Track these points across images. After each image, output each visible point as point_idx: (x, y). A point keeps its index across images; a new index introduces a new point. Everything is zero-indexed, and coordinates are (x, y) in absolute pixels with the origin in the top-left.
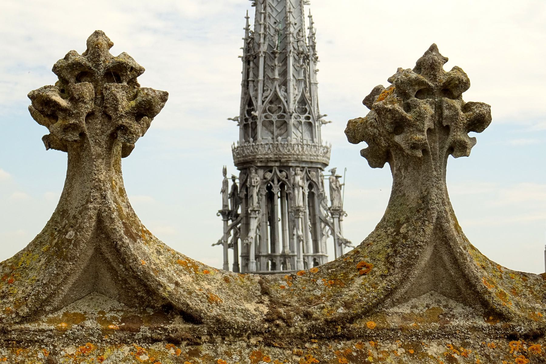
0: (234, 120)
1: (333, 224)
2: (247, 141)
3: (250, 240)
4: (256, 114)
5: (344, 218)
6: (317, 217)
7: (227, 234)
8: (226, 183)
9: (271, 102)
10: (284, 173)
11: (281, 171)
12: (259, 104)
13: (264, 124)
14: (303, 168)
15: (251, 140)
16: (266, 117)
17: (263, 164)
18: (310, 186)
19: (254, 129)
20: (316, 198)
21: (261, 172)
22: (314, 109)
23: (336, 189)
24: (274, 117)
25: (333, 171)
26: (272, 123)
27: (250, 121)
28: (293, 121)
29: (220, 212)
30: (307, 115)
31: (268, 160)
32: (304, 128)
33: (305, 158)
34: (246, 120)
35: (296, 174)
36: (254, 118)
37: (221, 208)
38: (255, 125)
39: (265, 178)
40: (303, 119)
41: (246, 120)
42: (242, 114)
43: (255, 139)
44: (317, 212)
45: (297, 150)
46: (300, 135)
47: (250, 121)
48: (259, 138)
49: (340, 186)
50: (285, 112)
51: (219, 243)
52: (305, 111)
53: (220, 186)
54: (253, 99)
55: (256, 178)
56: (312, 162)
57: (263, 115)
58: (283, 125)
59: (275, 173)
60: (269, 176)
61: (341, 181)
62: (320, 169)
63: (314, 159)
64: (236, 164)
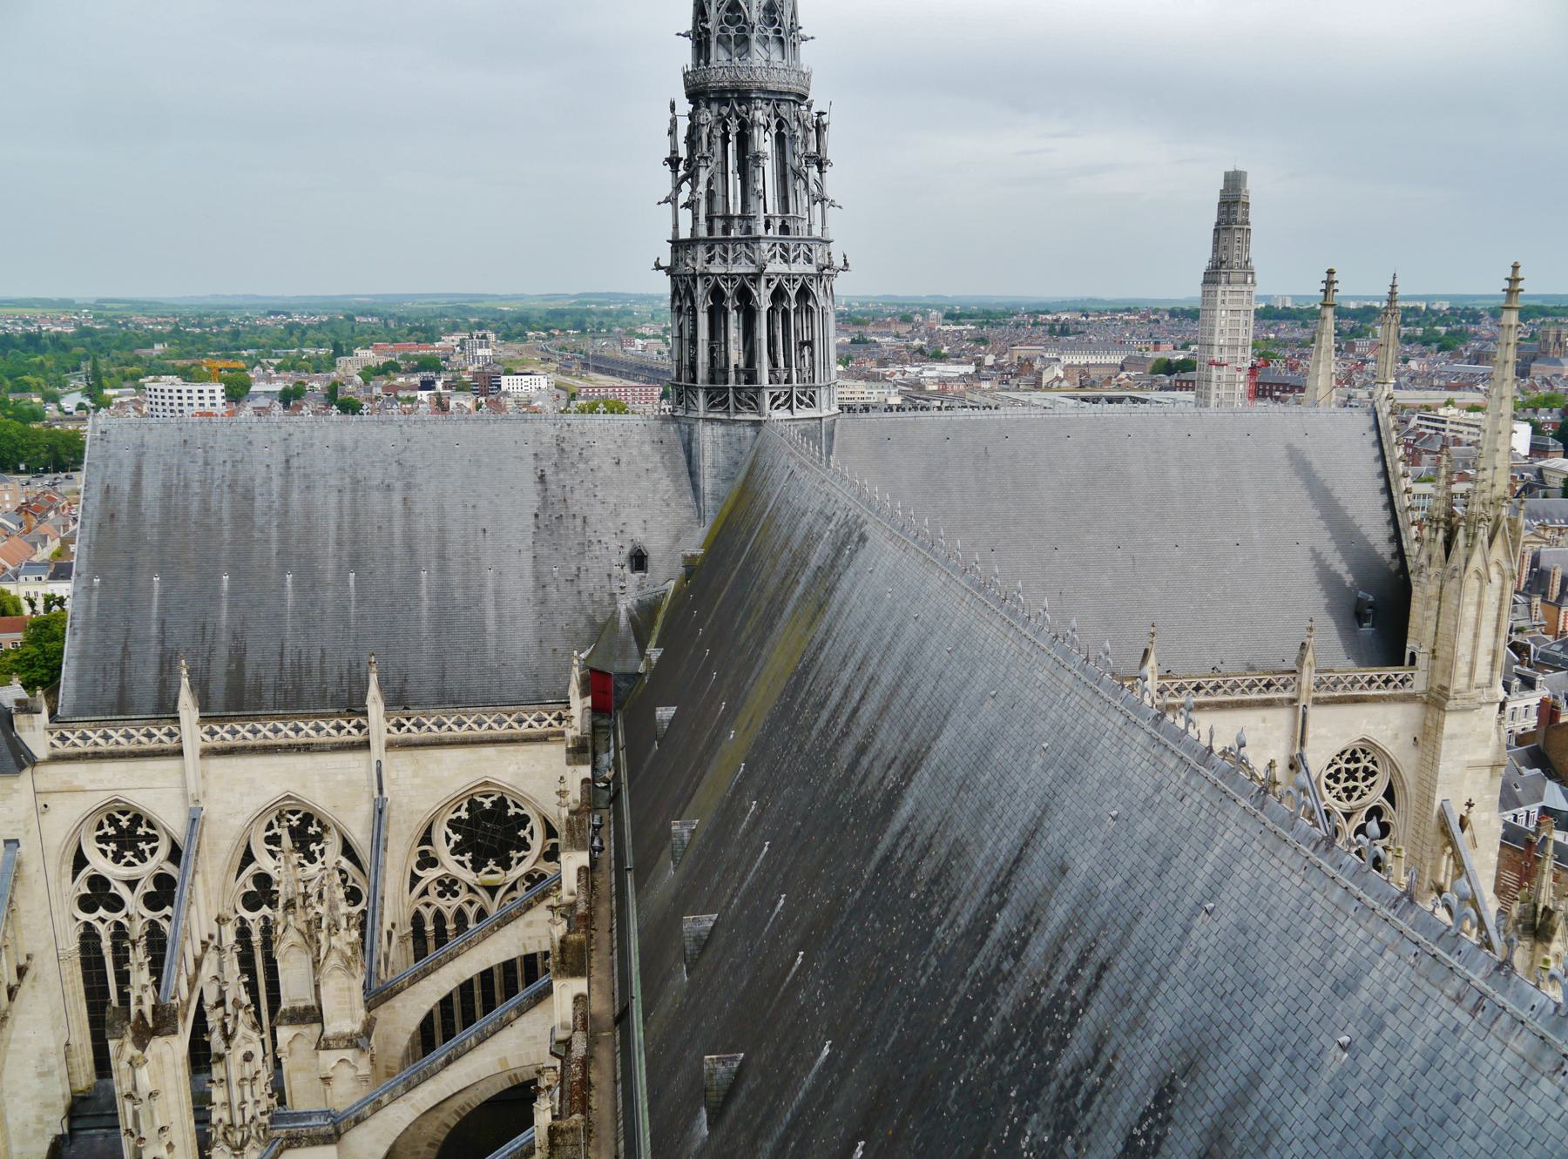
0: (684, 36)
1: (807, 175)
2: (698, 65)
3: (698, 196)
4: (709, 26)
5: (827, 168)
6: (788, 167)
7: (677, 188)
8: (674, 123)
9: (729, 9)
10: (744, 108)
11: (740, 105)
12: (712, 12)
13: (719, 40)
14: (770, 100)
15: (702, 61)
16: (721, 30)
17: (717, 95)
18: (779, 126)
19: (708, 49)
20: (787, 141)
21: (714, 107)
22: (787, 20)
23: (820, 128)
24: (732, 31)
25: (809, 107)
26: (729, 37)
27: (704, 35)
28: (754, 37)
29: (667, 159)
30: (776, 26)
31: (723, 90)
32: (774, 47)
33: (771, 87)
34: (699, 35)
35: (756, 108)
36: (707, 31)
37: (668, 156)
38: (708, 41)
39: (720, 114)
40: (770, 33)
41: (699, 35)
42: (695, 27)
43: (707, 63)
44: (788, 161)
45: (760, 76)
46: (765, 55)
47: (704, 35)
48: (712, 60)
49: (824, 126)
50: (745, 22)
51: (665, 202)
52: (773, 22)
53: (668, 125)
54: (706, 5)
55: (707, 116)
56: (781, 93)
57: (718, 28)
58: (743, 41)
59: (733, 107)
60: (725, 111)
61: (825, 119)
62: (795, 102)
63: (784, 88)
64: (688, 96)
